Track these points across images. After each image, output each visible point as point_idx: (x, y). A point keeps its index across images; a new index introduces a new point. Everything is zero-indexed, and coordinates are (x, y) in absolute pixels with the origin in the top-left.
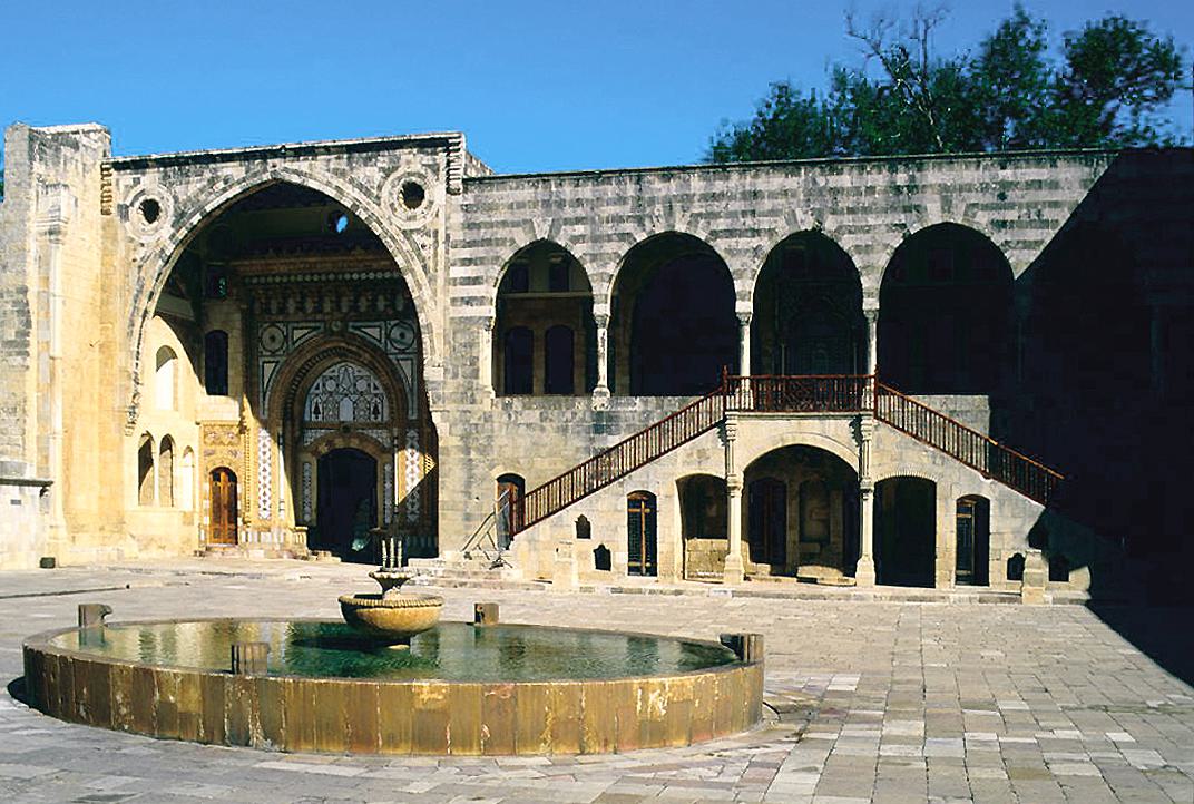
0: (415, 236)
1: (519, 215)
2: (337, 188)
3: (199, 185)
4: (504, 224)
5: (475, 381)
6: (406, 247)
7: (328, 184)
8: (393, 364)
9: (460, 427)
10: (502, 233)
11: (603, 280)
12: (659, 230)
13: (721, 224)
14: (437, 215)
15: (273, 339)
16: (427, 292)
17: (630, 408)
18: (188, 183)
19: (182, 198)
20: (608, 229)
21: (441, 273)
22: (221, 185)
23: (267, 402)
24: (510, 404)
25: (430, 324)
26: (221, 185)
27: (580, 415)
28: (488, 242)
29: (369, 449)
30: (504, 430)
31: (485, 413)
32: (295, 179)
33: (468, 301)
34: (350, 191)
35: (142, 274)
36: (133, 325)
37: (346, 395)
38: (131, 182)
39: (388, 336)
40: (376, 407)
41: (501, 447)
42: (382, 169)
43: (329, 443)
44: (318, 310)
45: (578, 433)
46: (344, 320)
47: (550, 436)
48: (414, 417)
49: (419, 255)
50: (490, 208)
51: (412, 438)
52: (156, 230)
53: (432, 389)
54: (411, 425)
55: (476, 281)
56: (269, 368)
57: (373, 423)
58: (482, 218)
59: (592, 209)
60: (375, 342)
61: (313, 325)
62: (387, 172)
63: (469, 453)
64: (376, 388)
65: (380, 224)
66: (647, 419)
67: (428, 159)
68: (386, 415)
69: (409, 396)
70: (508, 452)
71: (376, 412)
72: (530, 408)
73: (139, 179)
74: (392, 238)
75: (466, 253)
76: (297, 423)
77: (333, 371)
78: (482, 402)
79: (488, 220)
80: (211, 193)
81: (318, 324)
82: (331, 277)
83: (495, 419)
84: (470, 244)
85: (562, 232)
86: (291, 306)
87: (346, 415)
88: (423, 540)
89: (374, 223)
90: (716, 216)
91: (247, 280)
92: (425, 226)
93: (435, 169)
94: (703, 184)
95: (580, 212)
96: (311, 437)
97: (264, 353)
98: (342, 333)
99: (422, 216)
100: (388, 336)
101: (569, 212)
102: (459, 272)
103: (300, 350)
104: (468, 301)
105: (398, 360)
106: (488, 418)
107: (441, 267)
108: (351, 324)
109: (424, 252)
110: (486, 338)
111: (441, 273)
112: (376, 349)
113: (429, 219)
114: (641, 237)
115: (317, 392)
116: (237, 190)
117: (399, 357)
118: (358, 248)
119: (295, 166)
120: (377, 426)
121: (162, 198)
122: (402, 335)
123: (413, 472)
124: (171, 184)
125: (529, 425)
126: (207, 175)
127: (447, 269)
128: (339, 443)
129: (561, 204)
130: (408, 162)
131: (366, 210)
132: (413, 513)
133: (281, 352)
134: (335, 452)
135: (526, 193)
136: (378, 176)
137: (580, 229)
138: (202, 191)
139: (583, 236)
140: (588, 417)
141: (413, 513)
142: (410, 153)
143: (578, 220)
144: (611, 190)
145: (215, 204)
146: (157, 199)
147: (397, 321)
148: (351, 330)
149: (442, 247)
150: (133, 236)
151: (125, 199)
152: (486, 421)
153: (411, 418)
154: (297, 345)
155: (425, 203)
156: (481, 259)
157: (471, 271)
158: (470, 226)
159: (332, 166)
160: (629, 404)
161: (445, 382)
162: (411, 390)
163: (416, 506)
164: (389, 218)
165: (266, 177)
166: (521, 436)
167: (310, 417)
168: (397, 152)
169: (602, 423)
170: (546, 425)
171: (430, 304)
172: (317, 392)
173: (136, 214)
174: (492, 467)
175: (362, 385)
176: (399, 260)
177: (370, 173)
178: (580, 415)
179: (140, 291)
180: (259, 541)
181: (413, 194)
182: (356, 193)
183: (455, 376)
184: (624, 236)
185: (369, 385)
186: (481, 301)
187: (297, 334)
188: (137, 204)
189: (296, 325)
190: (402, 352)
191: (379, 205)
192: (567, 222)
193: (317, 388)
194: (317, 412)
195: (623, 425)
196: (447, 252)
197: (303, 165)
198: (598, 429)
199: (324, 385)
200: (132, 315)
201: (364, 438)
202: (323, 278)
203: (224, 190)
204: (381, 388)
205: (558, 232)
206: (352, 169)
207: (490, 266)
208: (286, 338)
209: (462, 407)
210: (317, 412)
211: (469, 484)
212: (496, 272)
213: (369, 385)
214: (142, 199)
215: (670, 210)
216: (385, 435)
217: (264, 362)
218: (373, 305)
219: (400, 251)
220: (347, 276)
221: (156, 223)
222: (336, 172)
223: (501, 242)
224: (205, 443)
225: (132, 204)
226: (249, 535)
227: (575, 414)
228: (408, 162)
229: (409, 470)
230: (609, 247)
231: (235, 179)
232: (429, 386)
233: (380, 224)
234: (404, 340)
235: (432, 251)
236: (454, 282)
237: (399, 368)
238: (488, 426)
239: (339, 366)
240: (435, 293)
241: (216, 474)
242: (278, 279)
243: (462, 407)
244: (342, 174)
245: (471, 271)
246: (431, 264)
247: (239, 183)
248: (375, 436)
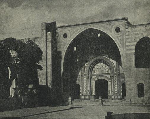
29: (106, 79)
43: (97, 78)
54: (115, 74)
55: (132, 46)
71: (107, 72)
105: (112, 61)
110: (133, 56)
123: (116, 83)
128: (100, 78)
134: (98, 80)
141: (116, 91)
153: (115, 72)
163: (117, 90)
175: (104, 66)
194: (95, 72)
210: (95, 72)
231: (83, 29)
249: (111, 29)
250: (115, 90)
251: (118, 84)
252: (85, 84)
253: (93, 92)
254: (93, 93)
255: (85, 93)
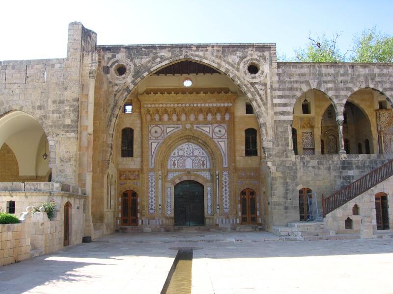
0: (257, 86)
1: (302, 79)
2: (218, 63)
3: (147, 60)
4: (297, 82)
5: (287, 148)
6: (252, 90)
7: (213, 61)
8: (216, 144)
9: (281, 167)
10: (296, 86)
11: (341, 106)
12: (363, 86)
13: (387, 86)
14: (266, 77)
15: (156, 132)
16: (263, 108)
17: (357, 159)
18: (142, 58)
19: (138, 64)
20: (341, 86)
21: (269, 101)
22: (159, 60)
23: (153, 159)
24: (304, 158)
25: (265, 123)
26: (159, 60)
27: (335, 162)
28: (291, 89)
29: (200, 181)
30: (302, 169)
31: (292, 162)
32: (197, 59)
33: (283, 113)
34: (224, 65)
35: (116, 98)
36: (111, 122)
37: (189, 157)
38: (110, 56)
39: (213, 131)
40: (203, 162)
41: (301, 176)
42: (239, 57)
43: (180, 178)
44: (178, 120)
45: (335, 170)
46: (192, 124)
47: (323, 172)
48: (226, 166)
49: (258, 93)
50: (291, 75)
51: (225, 175)
52: (124, 78)
53: (267, 151)
55: (285, 105)
56: (154, 145)
57: (202, 169)
58: (287, 79)
59: (334, 78)
60: (207, 133)
61: (176, 126)
62: (242, 58)
63: (285, 180)
64: (203, 154)
65: (239, 79)
66: (364, 164)
67: (259, 54)
68: (208, 164)
69: (224, 157)
70: (304, 179)
71: (203, 164)
72: (313, 159)
73: (115, 55)
74: (245, 86)
75: (280, 93)
76: (166, 169)
77: (182, 147)
78: (291, 157)
79: (289, 80)
80: (153, 63)
81: (179, 126)
82: (188, 105)
83: (298, 164)
84: (284, 90)
85: (322, 86)
86: (166, 117)
87: (189, 165)
88: (231, 221)
89: (236, 79)
90: (385, 82)
91: (145, 106)
92: (260, 81)
93: (265, 59)
94: (379, 70)
95: (329, 78)
96: (171, 176)
97: (152, 138)
98: (191, 129)
99: (258, 78)
100: (213, 131)
101: (325, 79)
102: (276, 101)
103: (170, 137)
104: (283, 113)
105: (218, 142)
106: (294, 164)
107: (269, 98)
108: (195, 126)
109: (261, 92)
111: (269, 101)
112: (207, 136)
113: (262, 78)
114: (356, 89)
115: (174, 156)
116: (167, 62)
117: (219, 140)
118: (202, 92)
119: (197, 53)
120: (204, 170)
121: (128, 64)
122: (220, 131)
123: (226, 190)
124: (132, 59)
125: (313, 167)
126: (151, 55)
127: (272, 101)
128: (185, 178)
129: (321, 75)
130: (251, 55)
131: (232, 73)
132: (226, 208)
133: (160, 138)
134: (182, 183)
135: (306, 70)
136: (237, 60)
137: (330, 85)
138: (149, 62)
139: (332, 88)
140: (339, 163)
141: (226, 208)
142: (252, 51)
143: (329, 82)
144: (342, 71)
145: (156, 67)
146: (125, 64)
147: (217, 125)
148: (195, 128)
149: (269, 91)
150: (111, 80)
151: (108, 63)
152: (293, 165)
153: (224, 166)
154: (169, 134)
155: (260, 72)
156: (288, 96)
157: (283, 101)
158: (280, 82)
159: (215, 54)
160: (356, 157)
161: (273, 149)
162: (225, 154)
164: (243, 77)
165: (182, 57)
166: (310, 171)
167: (169, 166)
168: (246, 50)
169: (346, 165)
170: (321, 166)
171: (264, 114)
172: (174, 156)
173: (112, 70)
174: (297, 185)
175: (196, 153)
176: (249, 95)
177: (234, 58)
178: (335, 162)
179: (115, 106)
180: (149, 224)
181: (253, 69)
182: (227, 66)
183: (278, 145)
184: (348, 89)
185: (200, 153)
186: (288, 113)
187: (169, 130)
188: (114, 67)
189: (168, 126)
190: (219, 138)
191: (238, 71)
192: (325, 82)
193: (175, 154)
194: (174, 164)
195: (354, 166)
196: (271, 92)
197: (201, 54)
198: (344, 168)
199: (178, 153)
200: (111, 117)
201: (197, 176)
202: (184, 105)
203: (160, 62)
204: (205, 153)
205: (320, 86)
206: (225, 56)
207: (291, 99)
208: (163, 131)
209: (281, 159)
210: (174, 164)
211: (286, 193)
212: (294, 101)
213: (200, 153)
214: (116, 64)
215: (366, 81)
216: (207, 174)
217: (152, 142)
218: (205, 119)
219: (249, 91)
220: (195, 105)
221: (124, 76)
222: (217, 57)
223: (297, 89)
224: (120, 179)
225: (111, 66)
226: (144, 221)
227: (333, 162)
228: (251, 55)
229: (224, 189)
230: (343, 93)
232: (266, 150)
233: (239, 79)
234: (221, 133)
235: (264, 92)
236: (275, 105)
237: (218, 145)
238: (294, 167)
239: (185, 144)
240: (267, 109)
241: (125, 195)
242: (161, 106)
243: (281, 159)
244: (220, 58)
245: (283, 101)
246: (264, 97)
247: (168, 59)
248: (203, 175)
249: (238, 64)
250: (224, 205)
251: (230, 191)
252: (152, 191)
253: (169, 208)
254: (169, 212)
255: (152, 211)
